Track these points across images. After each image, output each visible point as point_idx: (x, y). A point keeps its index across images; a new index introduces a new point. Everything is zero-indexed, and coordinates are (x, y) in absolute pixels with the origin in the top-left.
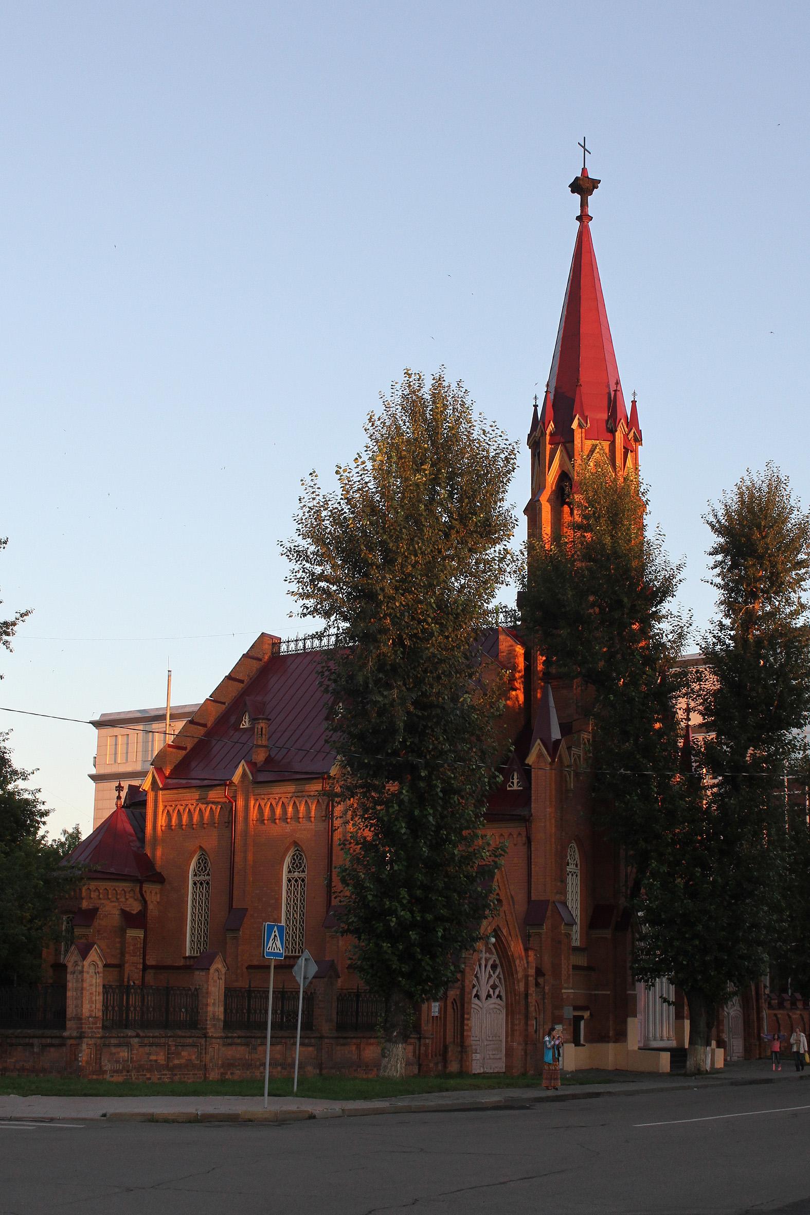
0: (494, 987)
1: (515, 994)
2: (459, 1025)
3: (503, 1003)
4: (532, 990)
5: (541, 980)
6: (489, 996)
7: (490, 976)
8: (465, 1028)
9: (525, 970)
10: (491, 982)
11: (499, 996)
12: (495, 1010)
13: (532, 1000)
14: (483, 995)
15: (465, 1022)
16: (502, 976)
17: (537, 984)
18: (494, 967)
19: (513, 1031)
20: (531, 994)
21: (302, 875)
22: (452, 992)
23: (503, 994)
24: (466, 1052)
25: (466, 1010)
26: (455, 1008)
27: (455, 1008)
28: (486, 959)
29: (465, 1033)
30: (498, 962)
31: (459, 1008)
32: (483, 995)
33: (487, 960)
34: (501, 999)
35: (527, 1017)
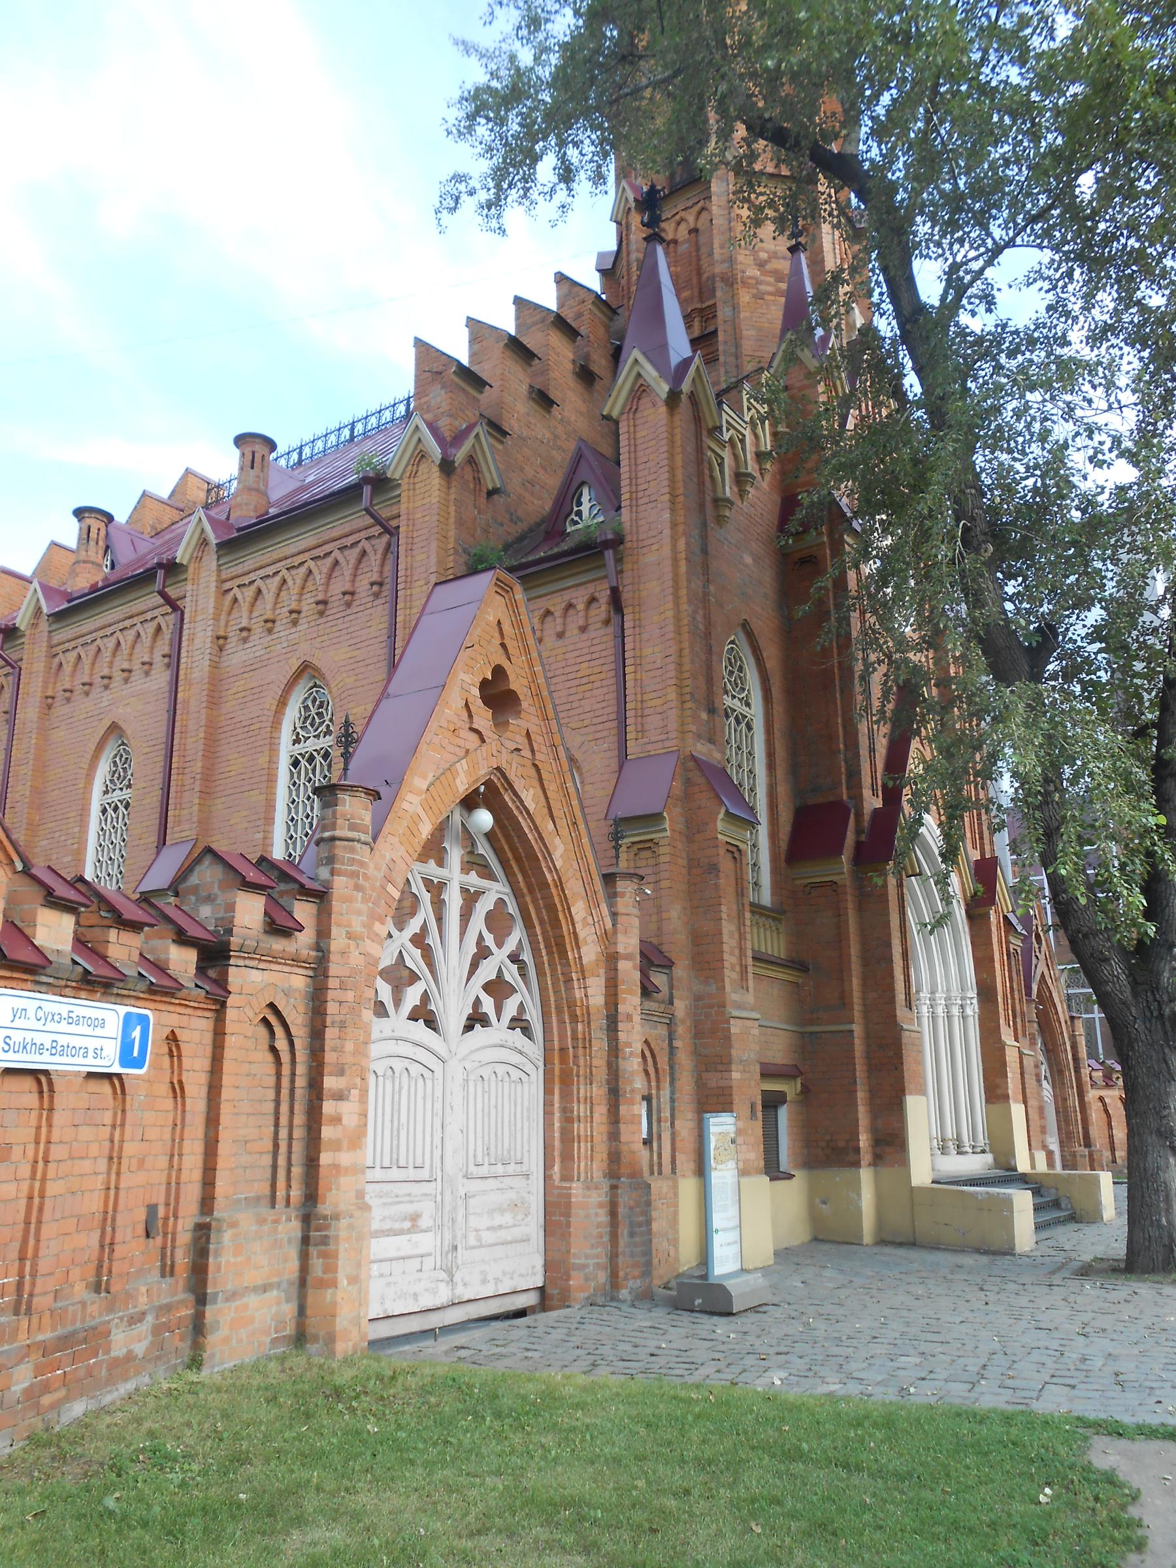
0: (498, 988)
1: (574, 1019)
2: (299, 1119)
3: (535, 1049)
4: (631, 1002)
5: (659, 979)
6: (476, 1020)
7: (483, 953)
8: (327, 1132)
9: (607, 938)
10: (487, 971)
11: (519, 1023)
12: (501, 1070)
13: (633, 1035)
14: (453, 1013)
15: (328, 1107)
16: (526, 956)
17: (647, 991)
18: (497, 922)
19: (568, 1138)
20: (629, 1018)
21: (126, 794)
22: (255, 976)
23: (534, 1016)
24: (325, 1241)
25: (330, 1057)
26: (281, 1044)
27: (281, 1044)
28: (464, 890)
29: (325, 1158)
30: (512, 908)
31: (298, 1044)
32: (453, 1013)
33: (471, 898)
34: (527, 1031)
35: (614, 1094)
